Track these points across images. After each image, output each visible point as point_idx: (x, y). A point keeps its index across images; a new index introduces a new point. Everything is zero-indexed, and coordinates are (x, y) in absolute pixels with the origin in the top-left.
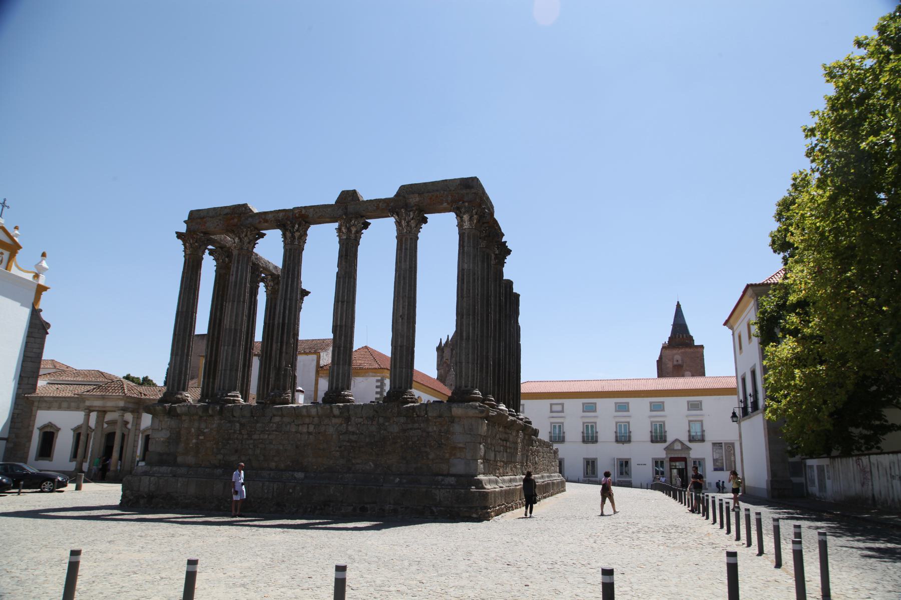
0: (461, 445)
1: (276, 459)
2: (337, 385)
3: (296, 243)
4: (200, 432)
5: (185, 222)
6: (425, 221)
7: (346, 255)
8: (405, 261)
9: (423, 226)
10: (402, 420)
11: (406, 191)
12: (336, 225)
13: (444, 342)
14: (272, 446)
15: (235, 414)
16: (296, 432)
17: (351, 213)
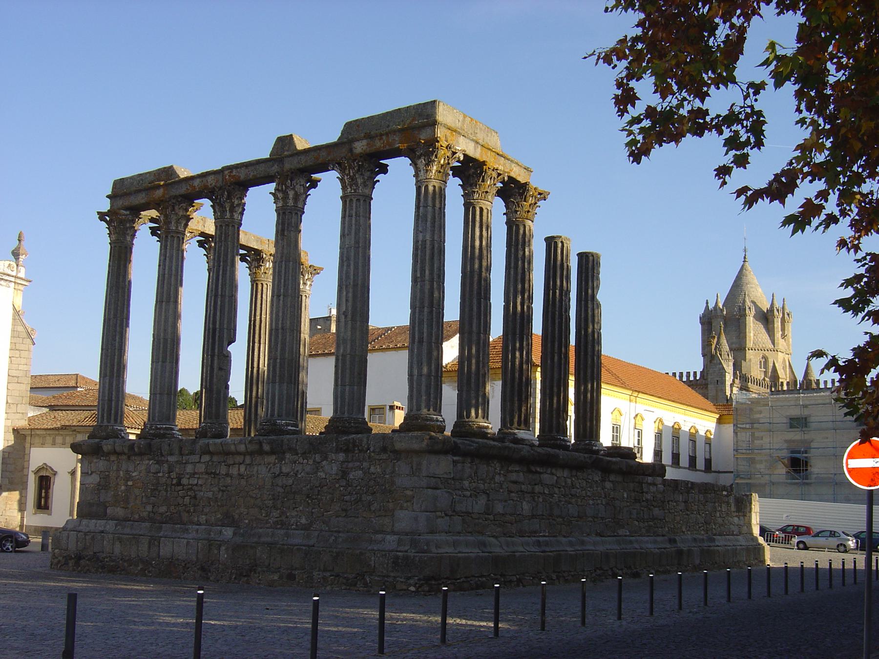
0: (409, 493)
1: (206, 510)
2: (273, 410)
3: (228, 215)
4: (128, 478)
5: (108, 197)
6: (384, 169)
7: (283, 230)
8: (349, 234)
9: (380, 177)
10: (341, 456)
11: (353, 129)
12: (272, 187)
13: (711, 306)
14: (202, 494)
15: (164, 453)
16: (227, 475)
17: (290, 170)
